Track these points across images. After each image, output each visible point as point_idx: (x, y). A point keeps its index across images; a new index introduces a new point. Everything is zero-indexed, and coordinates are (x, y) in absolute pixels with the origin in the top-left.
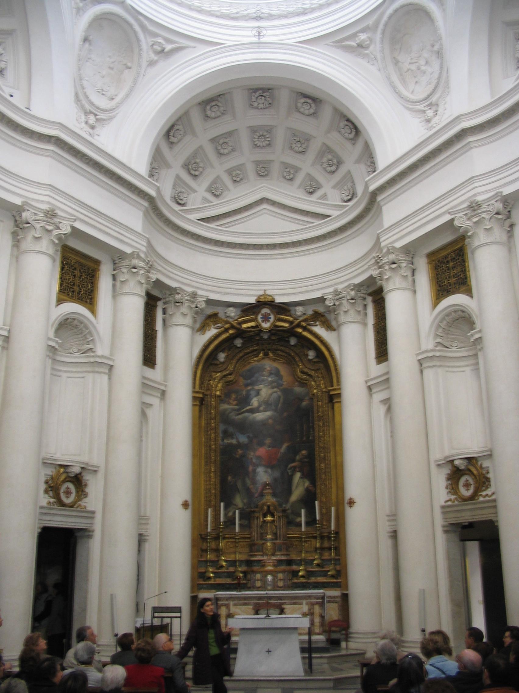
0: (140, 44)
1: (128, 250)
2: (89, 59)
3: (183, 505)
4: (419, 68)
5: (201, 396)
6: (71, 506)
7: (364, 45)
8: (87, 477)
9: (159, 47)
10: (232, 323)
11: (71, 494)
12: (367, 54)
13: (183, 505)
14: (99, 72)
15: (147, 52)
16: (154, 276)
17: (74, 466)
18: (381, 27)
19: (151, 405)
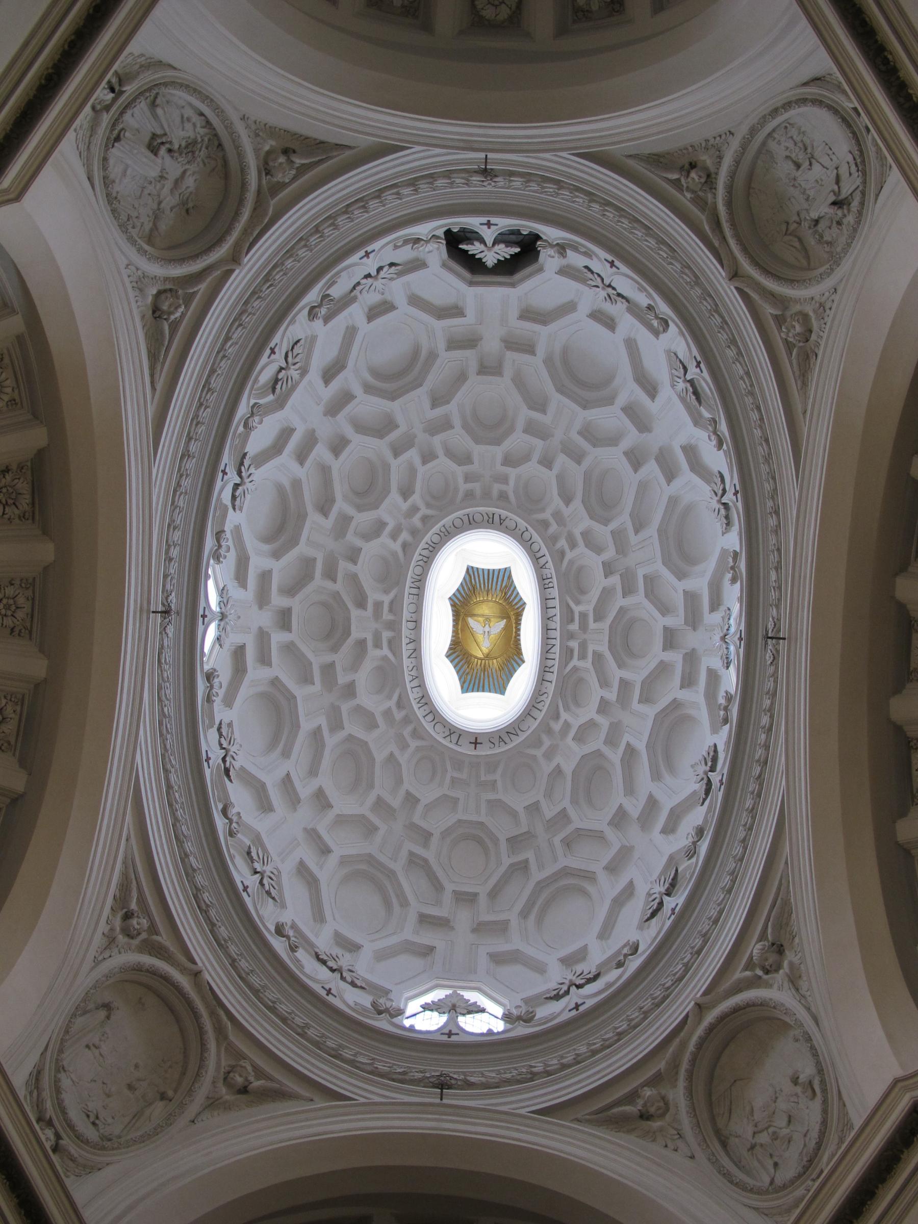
0: (206, 1055)
2: (94, 1045)
4: (775, 1137)
7: (652, 1110)
9: (241, 1076)
12: (661, 1129)
14: (104, 1083)
15: (214, 1082)
18: (684, 1066)
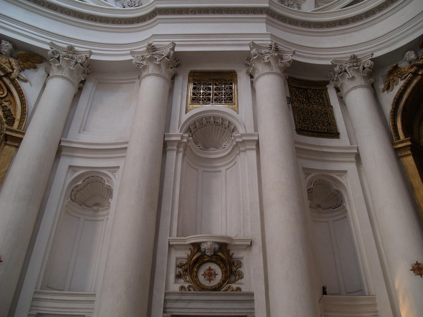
1: (248, 49)
3: (413, 270)
5: (409, 143)
6: (218, 288)
8: (237, 255)
10: (416, 63)
11: (217, 276)
13: (413, 270)
16: (288, 57)
17: (205, 242)
19: (345, 172)
